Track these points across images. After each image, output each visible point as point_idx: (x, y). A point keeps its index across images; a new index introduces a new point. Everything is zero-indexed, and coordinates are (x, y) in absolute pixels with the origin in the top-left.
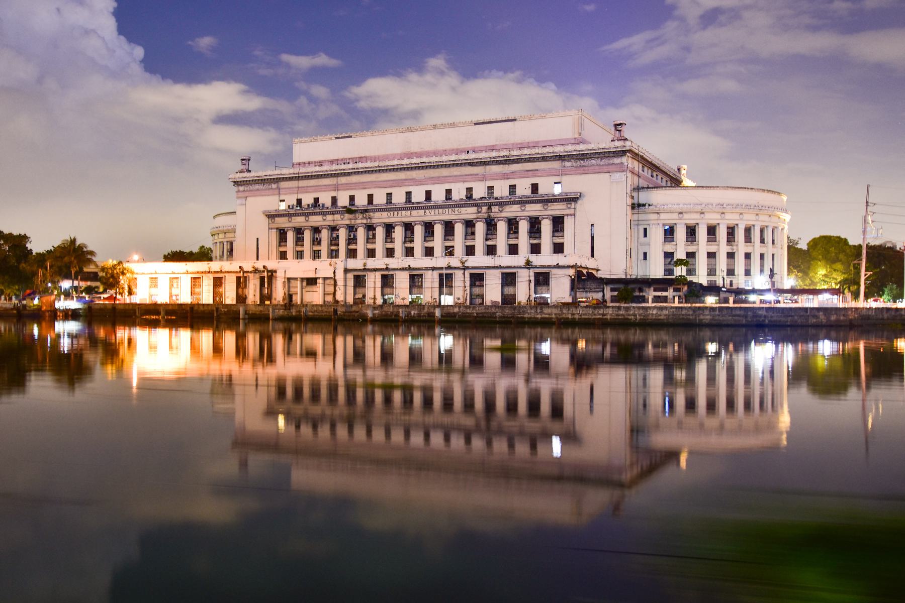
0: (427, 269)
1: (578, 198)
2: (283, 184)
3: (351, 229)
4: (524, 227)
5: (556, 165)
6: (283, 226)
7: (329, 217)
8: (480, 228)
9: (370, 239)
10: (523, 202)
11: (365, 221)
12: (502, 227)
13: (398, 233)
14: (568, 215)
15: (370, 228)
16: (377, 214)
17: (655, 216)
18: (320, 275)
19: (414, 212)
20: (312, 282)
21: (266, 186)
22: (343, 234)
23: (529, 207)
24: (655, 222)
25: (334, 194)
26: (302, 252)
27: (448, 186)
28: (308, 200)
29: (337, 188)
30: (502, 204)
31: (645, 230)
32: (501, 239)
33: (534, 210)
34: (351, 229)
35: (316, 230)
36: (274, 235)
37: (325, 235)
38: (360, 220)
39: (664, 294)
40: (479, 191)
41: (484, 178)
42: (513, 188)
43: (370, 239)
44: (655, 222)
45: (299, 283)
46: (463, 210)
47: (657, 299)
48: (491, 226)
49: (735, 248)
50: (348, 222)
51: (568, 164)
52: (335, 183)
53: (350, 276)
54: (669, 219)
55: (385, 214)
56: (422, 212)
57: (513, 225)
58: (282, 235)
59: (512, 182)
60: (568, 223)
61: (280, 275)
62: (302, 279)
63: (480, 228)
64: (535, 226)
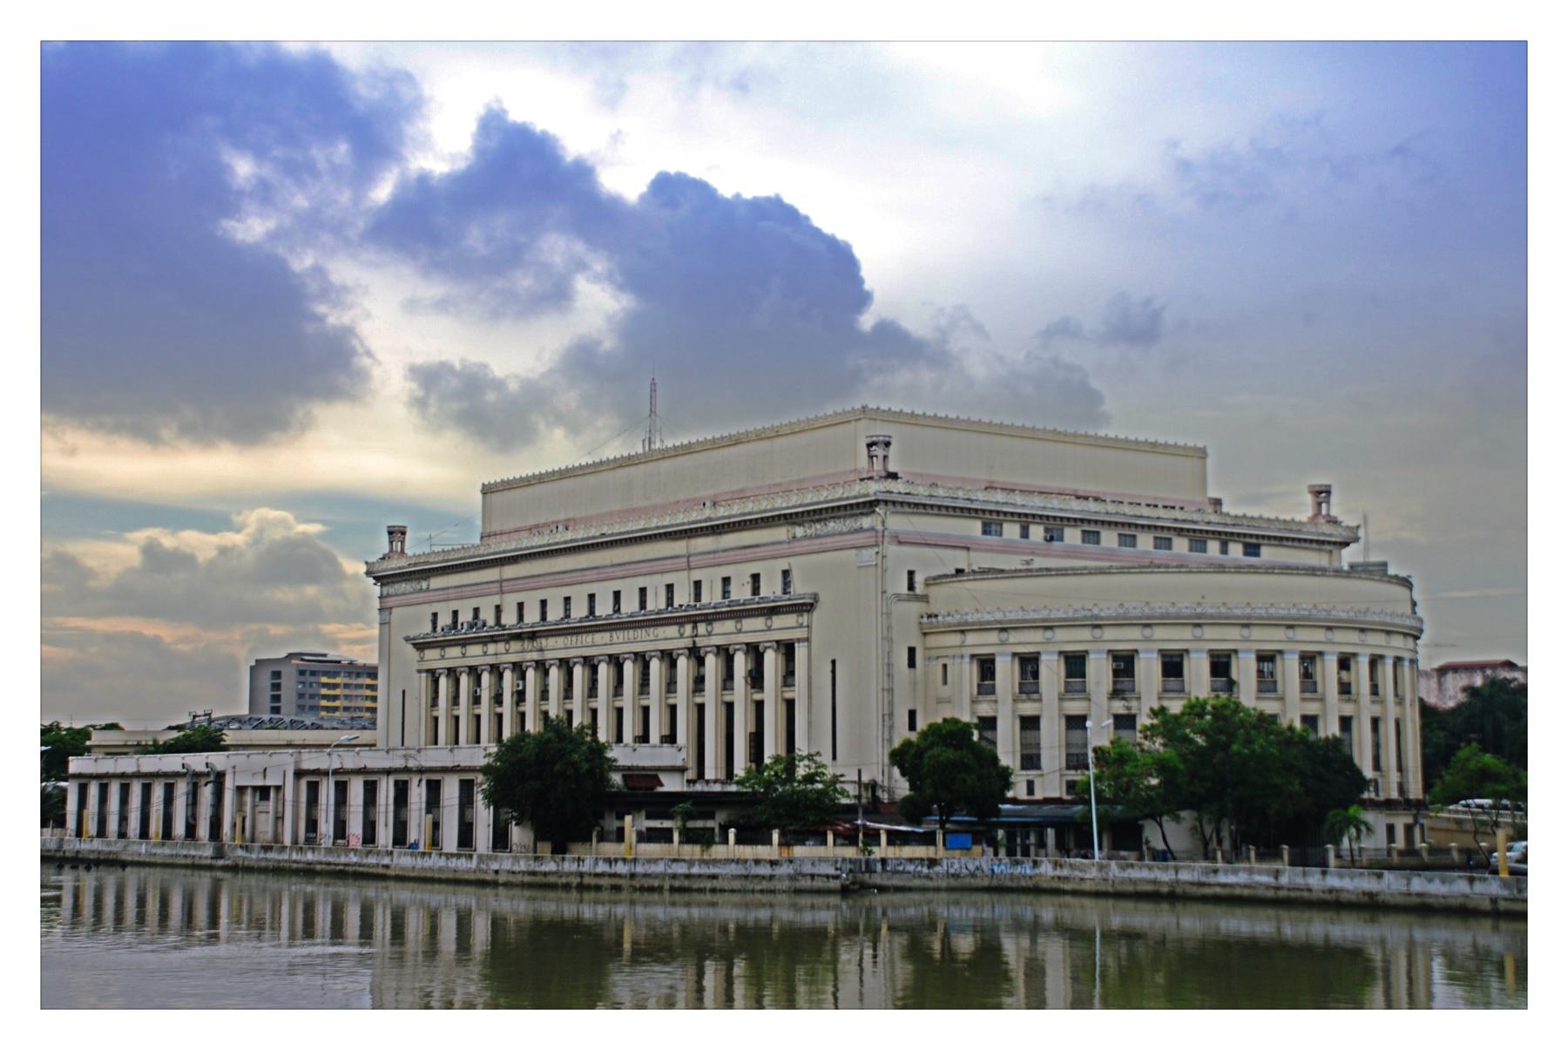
1: (812, 605)
2: (436, 582)
6: (433, 666)
7: (491, 648)
10: (738, 614)
11: (535, 656)
14: (799, 640)
16: (551, 642)
17: (955, 639)
19: (601, 638)
20: (263, 792)
29: (501, 586)
31: (945, 666)
35: (475, 672)
39: (667, 824)
44: (958, 651)
47: (648, 836)
49: (1134, 704)
51: (799, 531)
52: (497, 577)
55: (560, 641)
56: (604, 637)
60: (800, 652)
61: (229, 784)
62: (255, 788)
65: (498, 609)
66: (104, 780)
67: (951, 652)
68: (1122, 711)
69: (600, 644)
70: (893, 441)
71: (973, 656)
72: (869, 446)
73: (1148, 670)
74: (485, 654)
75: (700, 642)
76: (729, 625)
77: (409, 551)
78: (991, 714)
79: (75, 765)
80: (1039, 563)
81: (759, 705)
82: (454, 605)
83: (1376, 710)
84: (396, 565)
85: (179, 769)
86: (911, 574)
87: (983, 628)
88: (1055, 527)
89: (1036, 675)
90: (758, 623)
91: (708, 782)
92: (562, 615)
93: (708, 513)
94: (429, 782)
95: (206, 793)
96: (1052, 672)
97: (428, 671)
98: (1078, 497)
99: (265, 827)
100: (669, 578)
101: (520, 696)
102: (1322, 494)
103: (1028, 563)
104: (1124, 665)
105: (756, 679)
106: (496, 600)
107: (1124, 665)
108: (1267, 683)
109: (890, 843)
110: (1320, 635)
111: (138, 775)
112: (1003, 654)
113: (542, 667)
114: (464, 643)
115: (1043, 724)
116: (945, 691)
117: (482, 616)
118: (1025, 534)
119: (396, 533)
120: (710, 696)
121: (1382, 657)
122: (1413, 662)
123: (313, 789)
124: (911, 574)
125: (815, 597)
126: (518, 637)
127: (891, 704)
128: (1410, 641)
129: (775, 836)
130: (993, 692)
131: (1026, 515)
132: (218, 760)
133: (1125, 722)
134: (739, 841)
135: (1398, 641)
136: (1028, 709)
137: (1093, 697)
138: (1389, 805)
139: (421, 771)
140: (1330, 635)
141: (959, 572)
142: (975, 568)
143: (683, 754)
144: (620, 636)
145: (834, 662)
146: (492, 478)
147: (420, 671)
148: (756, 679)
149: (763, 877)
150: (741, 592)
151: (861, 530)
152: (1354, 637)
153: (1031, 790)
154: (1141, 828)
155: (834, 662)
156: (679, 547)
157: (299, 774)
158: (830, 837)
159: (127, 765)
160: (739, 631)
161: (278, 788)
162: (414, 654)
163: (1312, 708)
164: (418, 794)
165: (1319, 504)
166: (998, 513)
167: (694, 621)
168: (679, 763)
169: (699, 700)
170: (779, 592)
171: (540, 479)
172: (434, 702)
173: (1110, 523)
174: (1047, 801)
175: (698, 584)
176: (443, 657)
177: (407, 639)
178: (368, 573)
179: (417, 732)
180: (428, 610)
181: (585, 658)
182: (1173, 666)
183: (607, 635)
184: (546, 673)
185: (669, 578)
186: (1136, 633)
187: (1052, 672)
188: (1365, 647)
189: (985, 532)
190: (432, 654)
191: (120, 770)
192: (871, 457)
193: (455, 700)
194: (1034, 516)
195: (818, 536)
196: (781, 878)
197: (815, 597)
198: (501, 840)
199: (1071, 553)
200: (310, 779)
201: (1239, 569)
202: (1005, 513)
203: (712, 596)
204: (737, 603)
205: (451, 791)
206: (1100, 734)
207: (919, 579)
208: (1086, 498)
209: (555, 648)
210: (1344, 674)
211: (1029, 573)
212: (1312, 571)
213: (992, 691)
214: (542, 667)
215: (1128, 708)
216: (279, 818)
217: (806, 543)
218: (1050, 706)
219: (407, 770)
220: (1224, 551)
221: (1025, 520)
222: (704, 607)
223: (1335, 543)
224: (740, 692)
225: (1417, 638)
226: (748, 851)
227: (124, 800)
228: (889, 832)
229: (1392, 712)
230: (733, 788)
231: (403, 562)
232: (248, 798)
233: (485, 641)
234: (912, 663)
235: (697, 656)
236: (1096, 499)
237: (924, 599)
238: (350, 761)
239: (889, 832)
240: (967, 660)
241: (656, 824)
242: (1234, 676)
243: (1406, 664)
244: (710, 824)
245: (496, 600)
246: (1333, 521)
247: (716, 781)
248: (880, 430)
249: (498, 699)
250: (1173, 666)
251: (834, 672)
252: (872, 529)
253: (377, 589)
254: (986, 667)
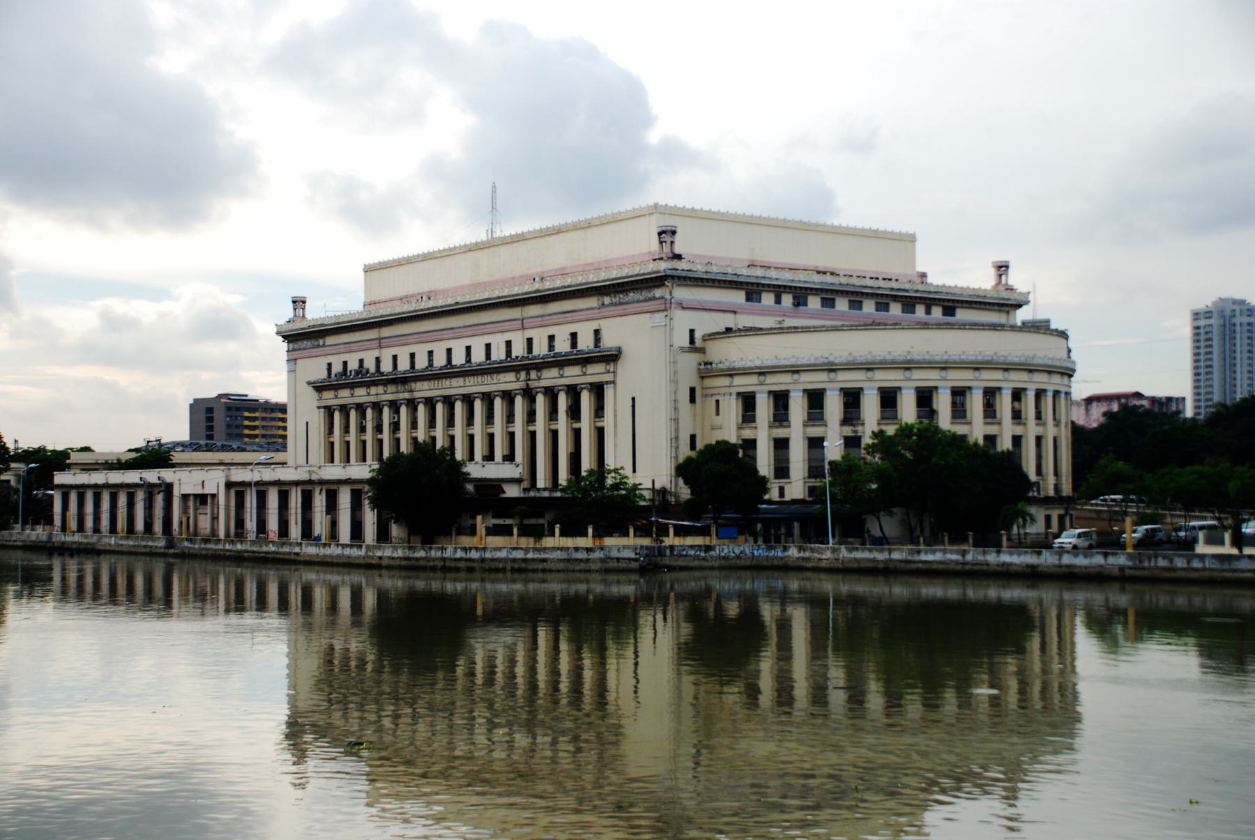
2: (330, 340)
5: (592, 302)
7: (373, 390)
10: (560, 362)
11: (407, 395)
14: (607, 383)
16: (419, 385)
17: (725, 381)
20: (202, 499)
24: (727, 390)
29: (380, 343)
31: (717, 401)
33: (572, 375)
35: (361, 408)
39: (508, 522)
44: (727, 390)
47: (493, 531)
49: (860, 428)
51: (607, 300)
54: (745, 383)
55: (426, 385)
56: (460, 381)
60: (609, 392)
62: (196, 496)
65: (378, 360)
66: (81, 489)
67: (722, 391)
68: (851, 434)
69: (457, 387)
70: (678, 230)
71: (738, 394)
72: (660, 234)
73: (870, 407)
74: (369, 394)
75: (533, 384)
76: (554, 372)
77: (309, 315)
78: (752, 437)
79: (60, 478)
80: (789, 322)
81: (577, 433)
82: (344, 357)
83: (1039, 431)
84: (299, 326)
85: (138, 481)
86: (692, 332)
87: (746, 372)
88: (801, 295)
89: (786, 407)
90: (576, 370)
91: (539, 490)
92: (426, 364)
93: (537, 286)
94: (328, 492)
95: (159, 500)
96: (798, 408)
97: (325, 407)
98: (819, 272)
99: (204, 523)
100: (508, 336)
101: (395, 427)
102: (1002, 268)
103: (780, 323)
104: (852, 399)
105: (574, 413)
106: (376, 353)
107: (852, 399)
108: (959, 412)
109: (676, 534)
110: (998, 375)
111: (107, 486)
112: (761, 392)
113: (412, 405)
114: (352, 386)
115: (792, 444)
116: (718, 420)
117: (366, 365)
118: (778, 301)
119: (299, 303)
120: (540, 426)
121: (1044, 391)
122: (1068, 394)
123: (240, 498)
124: (692, 332)
125: (619, 350)
126: (393, 381)
127: (677, 430)
128: (1066, 378)
129: (590, 531)
130: (754, 421)
131: (779, 286)
132: (168, 475)
133: (852, 442)
134: (562, 535)
135: (1056, 379)
136: (780, 433)
137: (829, 423)
138: (1047, 501)
139: (321, 482)
140: (1006, 374)
141: (729, 330)
142: (741, 327)
143: (520, 469)
144: (471, 380)
145: (633, 399)
146: (373, 259)
147: (319, 408)
148: (574, 413)
149: (581, 560)
150: (563, 346)
151: (654, 298)
152: (1024, 376)
153: (782, 493)
154: (863, 522)
155: (633, 399)
156: (515, 313)
157: (229, 485)
158: (631, 531)
159: (98, 478)
160: (562, 376)
161: (214, 496)
162: (315, 395)
163: (992, 430)
164: (319, 501)
165: (1000, 276)
166: (758, 284)
167: (528, 368)
168: (517, 476)
169: (531, 428)
170: (591, 346)
171: (408, 261)
172: (330, 431)
173: (842, 292)
174: (794, 502)
175: (530, 341)
176: (336, 397)
177: (309, 383)
178: (278, 333)
179: (317, 454)
180: (323, 362)
181: (445, 397)
182: (889, 399)
183: (461, 380)
184: (415, 409)
185: (508, 336)
186: (860, 375)
187: (798, 408)
188: (1032, 383)
189: (748, 299)
190: (328, 395)
191: (93, 482)
192: (661, 243)
193: (346, 429)
194: (785, 287)
195: (621, 304)
196: (594, 561)
197: (619, 350)
198: (383, 535)
199: (813, 315)
200: (237, 489)
201: (940, 326)
202: (763, 285)
203: (540, 349)
204: (560, 354)
205: (344, 499)
206: (834, 450)
207: (698, 335)
208: (825, 273)
209: (423, 390)
210: (1016, 404)
211: (781, 330)
212: (994, 327)
213: (753, 419)
214: (412, 405)
215: (856, 432)
216: (215, 518)
217: (612, 308)
218: (797, 431)
219: (310, 482)
220: (928, 312)
221: (778, 290)
222: (535, 358)
223: (1011, 306)
224: (562, 424)
225: (1071, 376)
226: (569, 542)
227: (97, 505)
228: (675, 526)
229: (1051, 431)
230: (558, 494)
231: (305, 325)
232: (191, 504)
233: (368, 385)
234: (692, 399)
235: (529, 395)
236: (832, 274)
237: (702, 350)
238: (267, 475)
239: (675, 526)
240: (734, 396)
241: (501, 522)
242: (935, 407)
243: (1063, 395)
244: (541, 521)
245: (376, 353)
246: (1010, 289)
247: (545, 489)
248: (668, 222)
249: (378, 428)
250: (889, 399)
251: (633, 406)
252: (662, 298)
253: (285, 346)
254: (748, 402)
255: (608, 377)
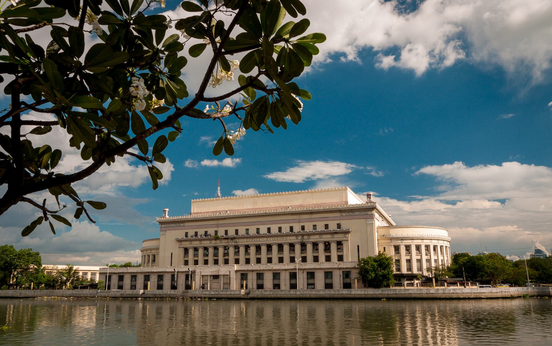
0: (283, 270)
2: (186, 224)
3: (226, 248)
4: (321, 247)
5: (337, 215)
8: (298, 248)
9: (237, 253)
11: (233, 244)
12: (309, 247)
13: (253, 250)
15: (237, 247)
16: (241, 240)
18: (221, 273)
19: (261, 239)
21: (178, 225)
22: (221, 251)
23: (324, 236)
25: (216, 229)
26: (207, 260)
27: (279, 225)
28: (201, 232)
29: (218, 226)
30: (309, 235)
32: (310, 253)
34: (226, 248)
35: (206, 249)
36: (182, 251)
37: (211, 251)
38: (231, 243)
40: (297, 228)
41: (299, 221)
42: (315, 226)
43: (237, 253)
45: (209, 277)
46: (288, 238)
47: (408, 285)
48: (303, 246)
50: (224, 244)
51: (344, 214)
53: (239, 274)
55: (245, 240)
56: (265, 239)
57: (315, 245)
58: (186, 250)
59: (315, 223)
62: (211, 276)
63: (298, 248)
64: (327, 247)
75: (304, 241)
145: (358, 246)
155: (358, 246)
162: (178, 243)
253: (160, 226)
255: (344, 239)
